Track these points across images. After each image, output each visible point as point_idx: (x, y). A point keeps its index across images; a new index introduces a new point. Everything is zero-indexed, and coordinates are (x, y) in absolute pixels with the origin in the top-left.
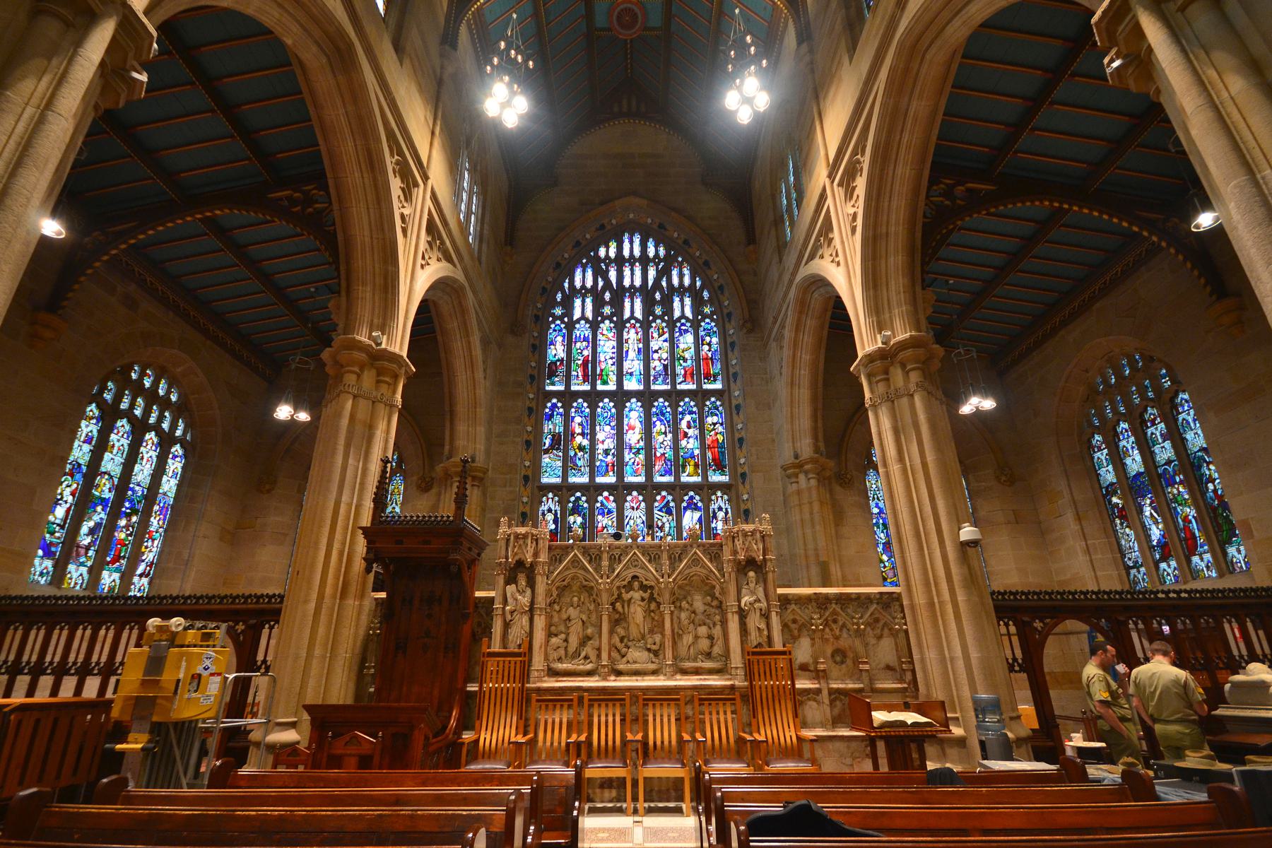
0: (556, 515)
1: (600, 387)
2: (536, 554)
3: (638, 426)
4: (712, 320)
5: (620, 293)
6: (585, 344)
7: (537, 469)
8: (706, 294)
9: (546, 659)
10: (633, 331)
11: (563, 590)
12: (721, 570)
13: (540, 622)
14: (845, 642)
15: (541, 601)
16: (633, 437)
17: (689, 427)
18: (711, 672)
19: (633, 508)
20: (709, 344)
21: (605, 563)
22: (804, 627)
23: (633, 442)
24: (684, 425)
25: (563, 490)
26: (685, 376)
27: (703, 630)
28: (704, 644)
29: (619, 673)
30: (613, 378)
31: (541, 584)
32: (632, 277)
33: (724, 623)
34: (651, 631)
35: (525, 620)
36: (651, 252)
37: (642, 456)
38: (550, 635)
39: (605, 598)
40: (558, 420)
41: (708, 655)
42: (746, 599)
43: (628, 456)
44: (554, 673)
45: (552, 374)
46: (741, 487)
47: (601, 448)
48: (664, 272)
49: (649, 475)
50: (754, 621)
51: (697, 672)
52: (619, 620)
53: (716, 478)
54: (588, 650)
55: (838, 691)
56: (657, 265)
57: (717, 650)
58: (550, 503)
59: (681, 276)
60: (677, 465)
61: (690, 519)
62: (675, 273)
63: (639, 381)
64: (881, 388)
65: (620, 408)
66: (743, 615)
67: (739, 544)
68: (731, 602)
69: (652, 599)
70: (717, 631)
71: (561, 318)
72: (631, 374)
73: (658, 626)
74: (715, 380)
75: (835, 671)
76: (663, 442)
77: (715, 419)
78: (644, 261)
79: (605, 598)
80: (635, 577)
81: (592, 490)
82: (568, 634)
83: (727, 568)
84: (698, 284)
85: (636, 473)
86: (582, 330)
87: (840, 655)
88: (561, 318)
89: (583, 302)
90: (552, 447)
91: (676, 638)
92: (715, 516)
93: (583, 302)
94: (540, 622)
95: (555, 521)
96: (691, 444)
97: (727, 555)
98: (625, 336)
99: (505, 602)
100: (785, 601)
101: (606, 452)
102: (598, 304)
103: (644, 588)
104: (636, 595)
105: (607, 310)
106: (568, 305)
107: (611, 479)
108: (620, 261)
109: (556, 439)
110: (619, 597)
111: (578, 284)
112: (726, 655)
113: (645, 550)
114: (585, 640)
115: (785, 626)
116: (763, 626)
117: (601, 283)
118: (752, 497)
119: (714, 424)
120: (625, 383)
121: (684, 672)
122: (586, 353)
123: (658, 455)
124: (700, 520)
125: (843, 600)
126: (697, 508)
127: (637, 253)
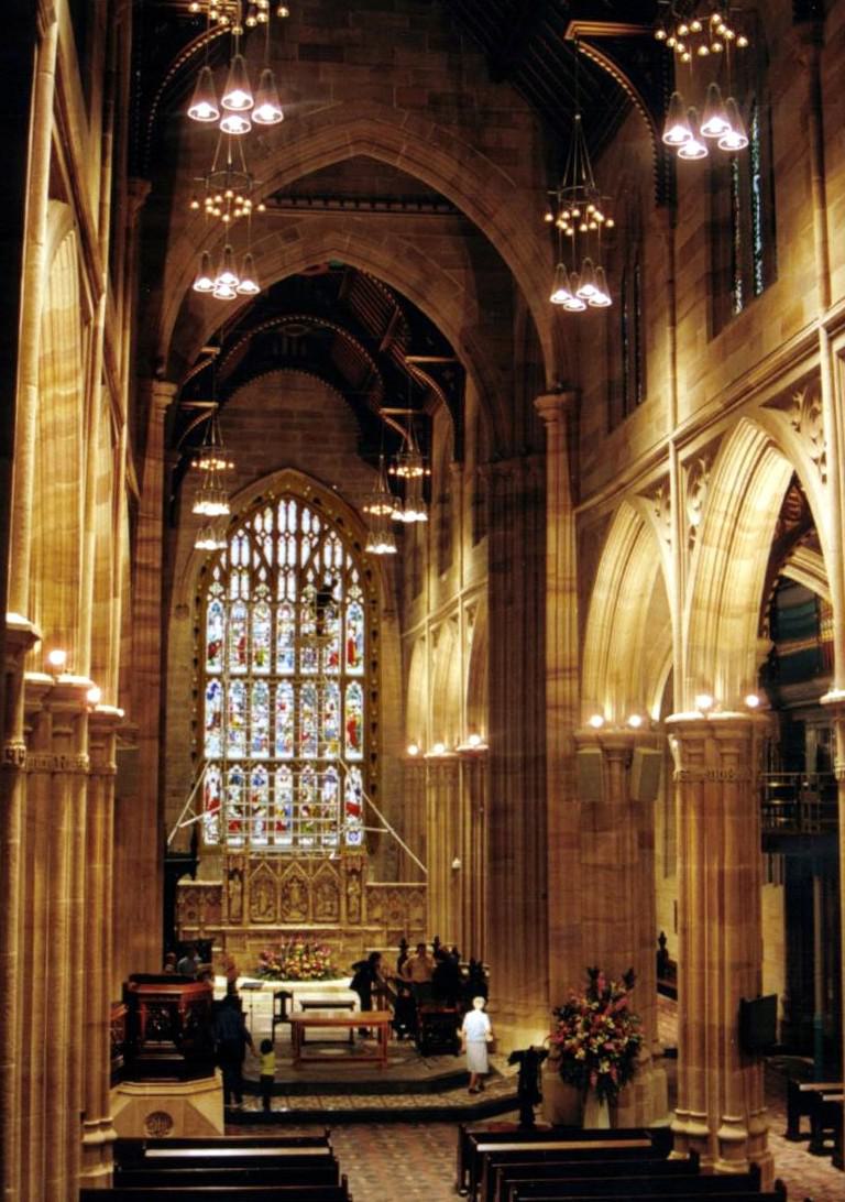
0: (218, 784)
1: (256, 670)
2: (244, 865)
3: (289, 708)
4: (359, 603)
5: (274, 571)
6: (241, 625)
7: (201, 745)
8: (355, 576)
9: (250, 915)
10: (286, 613)
11: (256, 882)
12: (339, 872)
13: (246, 899)
14: (400, 908)
15: (247, 890)
16: (284, 718)
17: (332, 708)
18: (330, 922)
19: (282, 780)
20: (355, 629)
21: (279, 870)
22: (378, 902)
23: (283, 722)
24: (327, 707)
25: (224, 764)
26: (332, 660)
27: (328, 903)
28: (328, 909)
29: (285, 922)
30: (267, 657)
31: (247, 880)
32: (287, 554)
33: (339, 900)
34: (302, 903)
35: (239, 899)
36: (306, 527)
37: (291, 735)
38: (251, 904)
39: (279, 887)
40: (218, 699)
41: (330, 915)
42: (351, 889)
43: (279, 735)
44: (253, 922)
45: (212, 655)
46: (371, 765)
47: (255, 726)
48: (317, 550)
49: (296, 753)
50: (354, 900)
51: (324, 922)
52: (286, 897)
53: (354, 755)
54: (270, 911)
55: (393, 932)
56: (311, 540)
57: (335, 911)
58: (211, 775)
59: (333, 554)
60: (322, 740)
61: (329, 790)
62: (327, 550)
63: (290, 664)
64: (434, 777)
65: (273, 688)
66: (348, 896)
67: (349, 861)
68: (343, 890)
69: (303, 887)
70: (335, 903)
71: (219, 596)
72: (283, 657)
73: (305, 900)
74: (357, 665)
75: (392, 922)
76: (309, 726)
77: (355, 702)
78: (299, 535)
79: (279, 887)
80: (294, 876)
81: (246, 765)
82: (259, 902)
83: (343, 874)
84: (349, 562)
85: (286, 749)
86: (239, 611)
87: (395, 915)
88: (219, 596)
89: (240, 579)
90: (214, 723)
91: (315, 906)
92: (348, 788)
93: (240, 579)
94: (246, 899)
95: (218, 790)
96: (332, 725)
97: (343, 867)
98: (279, 616)
99: (228, 888)
100: (370, 889)
101: (261, 730)
102: (254, 581)
103: (299, 881)
104: (295, 885)
105: (262, 588)
106: (225, 580)
107: (264, 755)
108: (275, 535)
109: (217, 717)
110: (286, 886)
111: (234, 561)
112: (339, 915)
113: (300, 863)
114: (269, 907)
115: (370, 901)
116: (357, 902)
117: (257, 560)
118: (379, 777)
119: (354, 707)
120: (278, 664)
121: (318, 922)
122: (242, 634)
123: (305, 734)
124: (336, 791)
125: (400, 889)
126: (334, 780)
127: (293, 528)
